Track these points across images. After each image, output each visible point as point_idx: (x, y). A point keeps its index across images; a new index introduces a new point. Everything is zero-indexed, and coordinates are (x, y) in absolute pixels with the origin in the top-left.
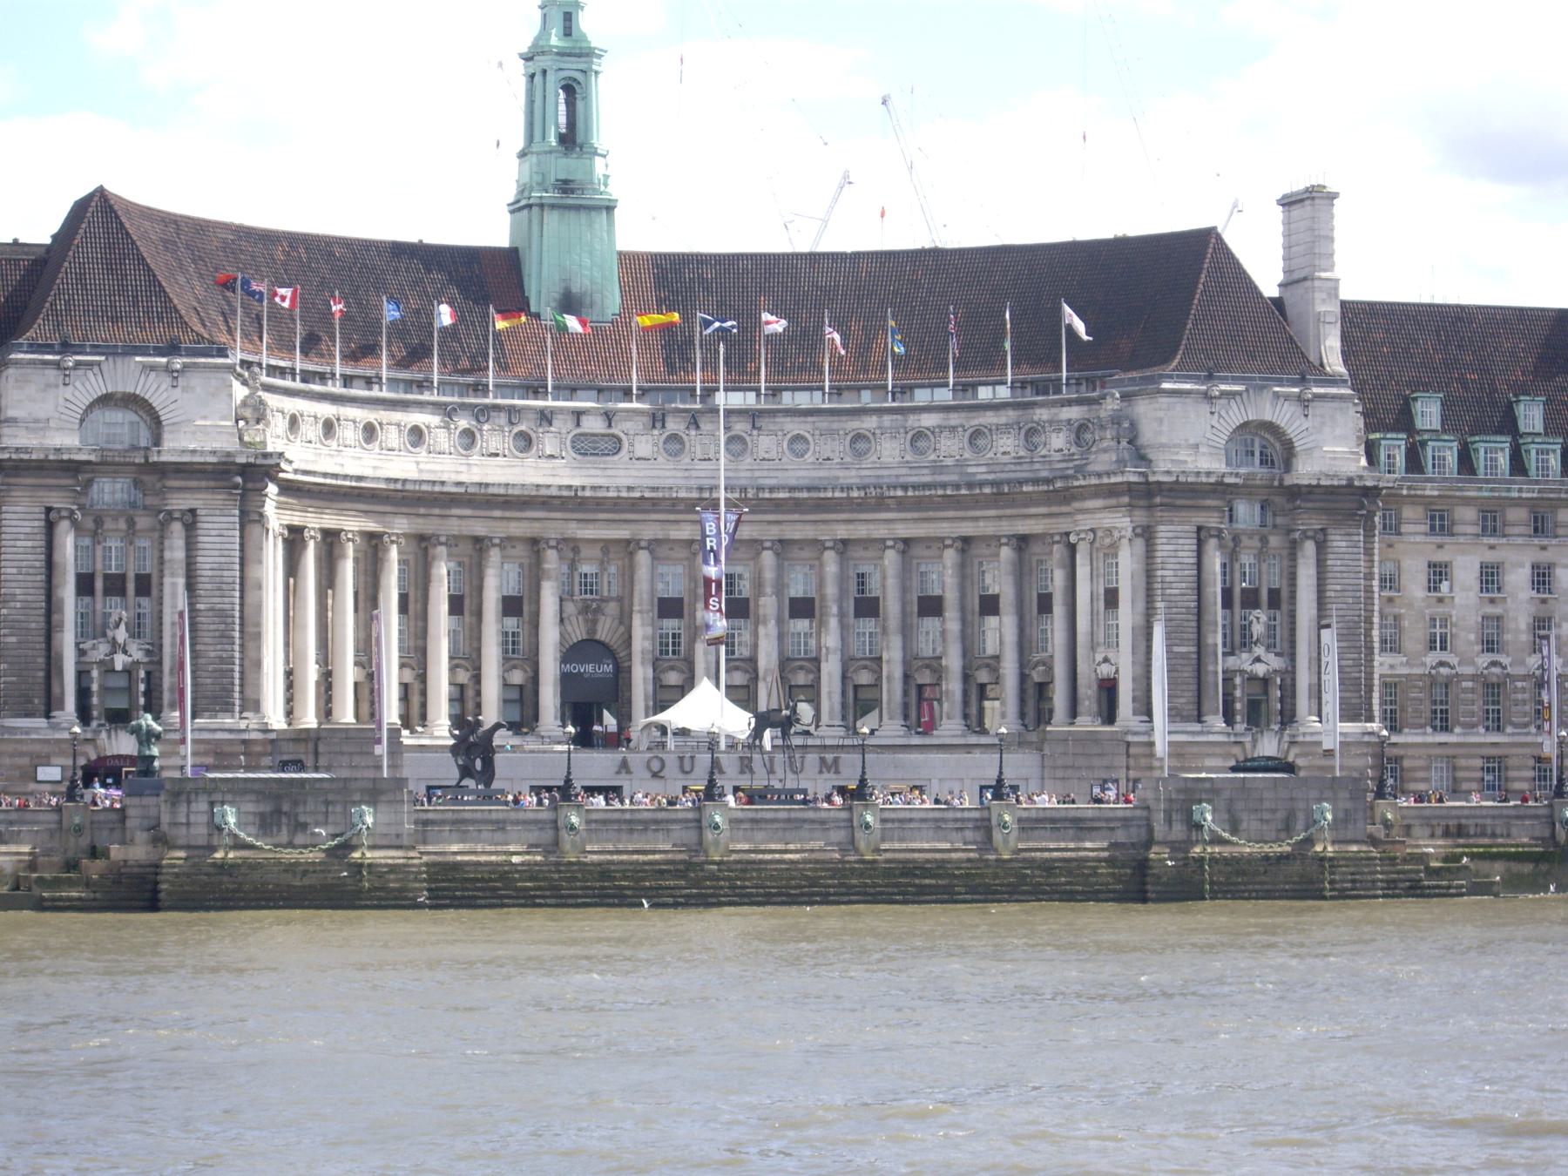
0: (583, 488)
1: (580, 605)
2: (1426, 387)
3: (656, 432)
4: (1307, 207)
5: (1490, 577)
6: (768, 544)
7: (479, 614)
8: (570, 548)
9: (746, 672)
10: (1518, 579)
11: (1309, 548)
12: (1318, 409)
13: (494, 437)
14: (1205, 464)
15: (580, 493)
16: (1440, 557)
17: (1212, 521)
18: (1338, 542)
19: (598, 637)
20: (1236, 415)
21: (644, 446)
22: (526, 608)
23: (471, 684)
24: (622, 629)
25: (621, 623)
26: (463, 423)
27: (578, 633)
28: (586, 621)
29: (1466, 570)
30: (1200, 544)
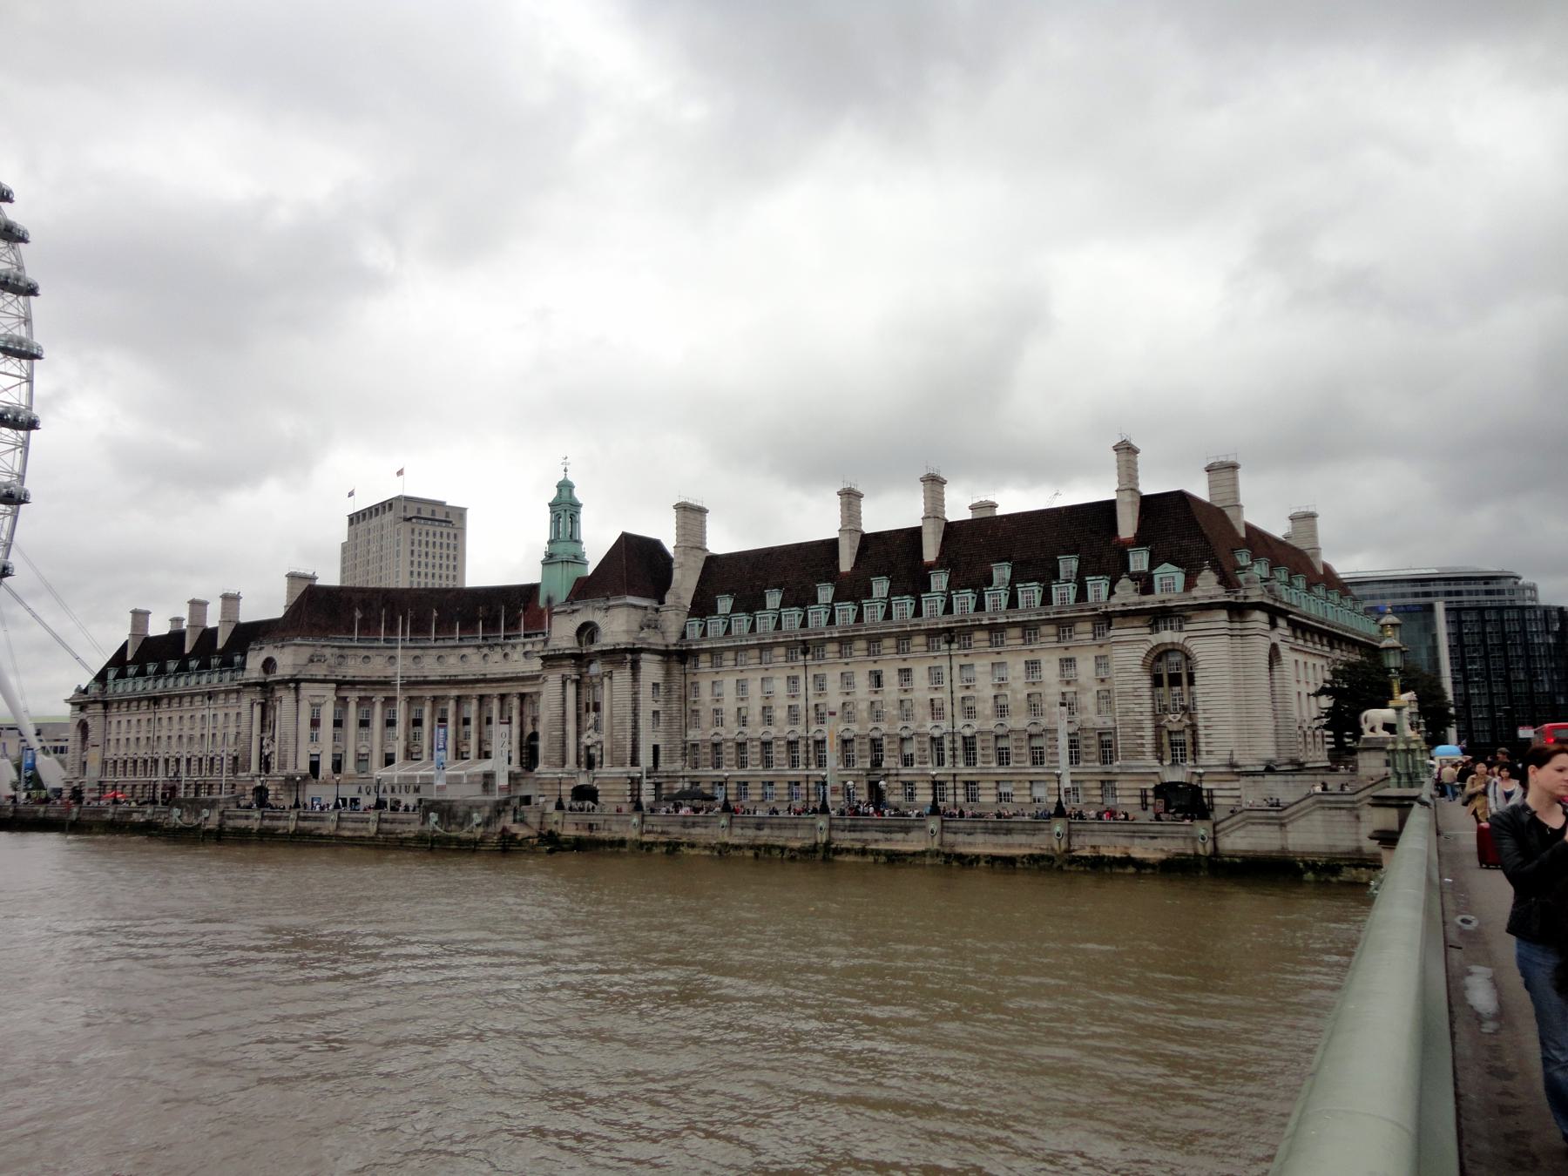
2: (730, 592)
4: (691, 515)
5: (741, 686)
8: (522, 696)
10: (754, 688)
11: (606, 680)
12: (611, 612)
13: (496, 655)
14: (565, 645)
16: (717, 678)
17: (567, 671)
18: (616, 676)
20: (579, 620)
26: (485, 651)
29: (729, 683)
30: (564, 683)
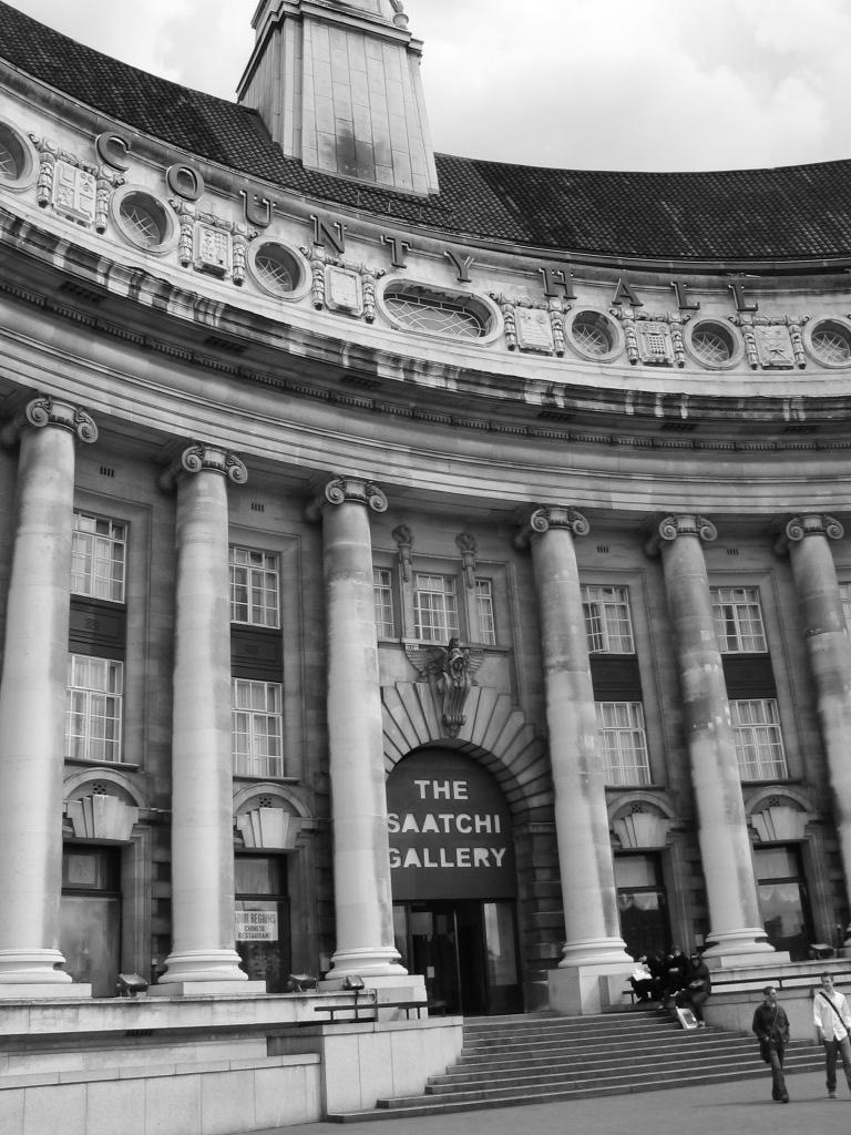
0: (426, 366)
1: (420, 661)
3: (557, 304)
6: (814, 523)
7: (167, 653)
9: (800, 808)
15: (420, 380)
19: (465, 734)
21: (536, 328)
22: (290, 660)
23: (145, 839)
24: (518, 719)
25: (516, 705)
27: (422, 729)
28: (438, 695)
